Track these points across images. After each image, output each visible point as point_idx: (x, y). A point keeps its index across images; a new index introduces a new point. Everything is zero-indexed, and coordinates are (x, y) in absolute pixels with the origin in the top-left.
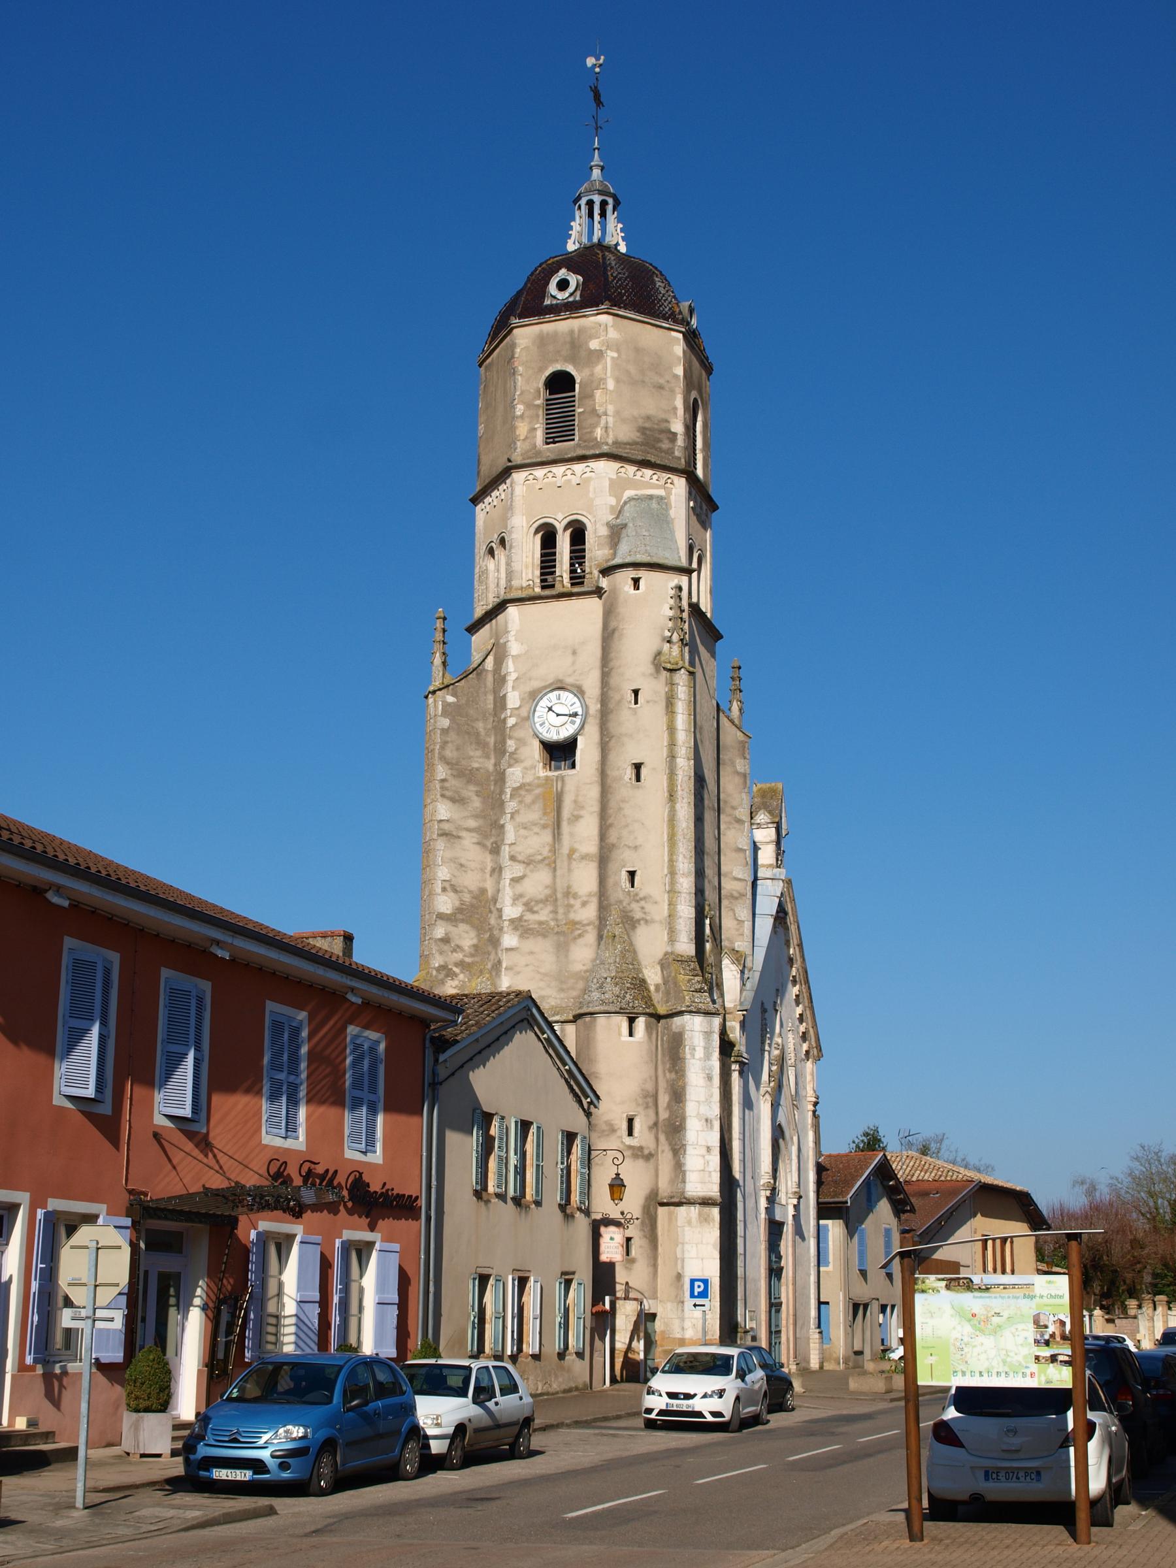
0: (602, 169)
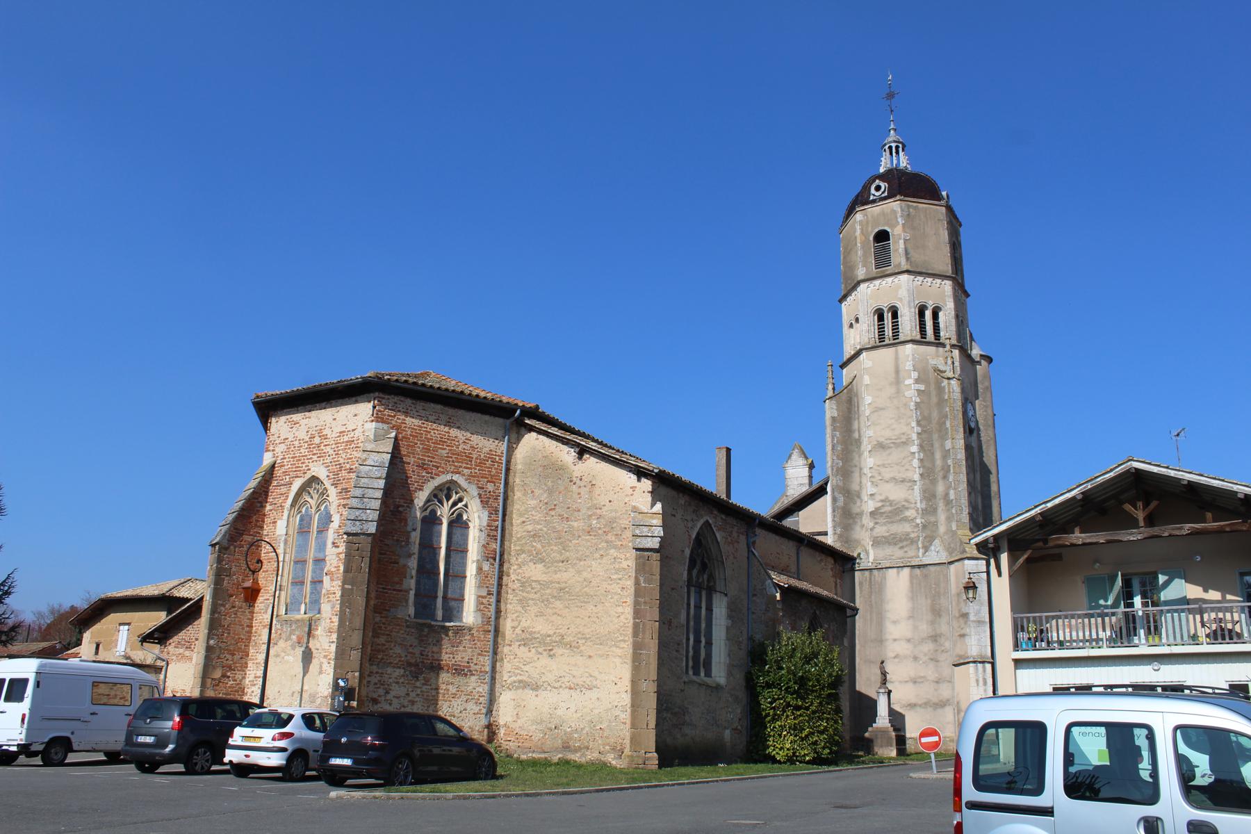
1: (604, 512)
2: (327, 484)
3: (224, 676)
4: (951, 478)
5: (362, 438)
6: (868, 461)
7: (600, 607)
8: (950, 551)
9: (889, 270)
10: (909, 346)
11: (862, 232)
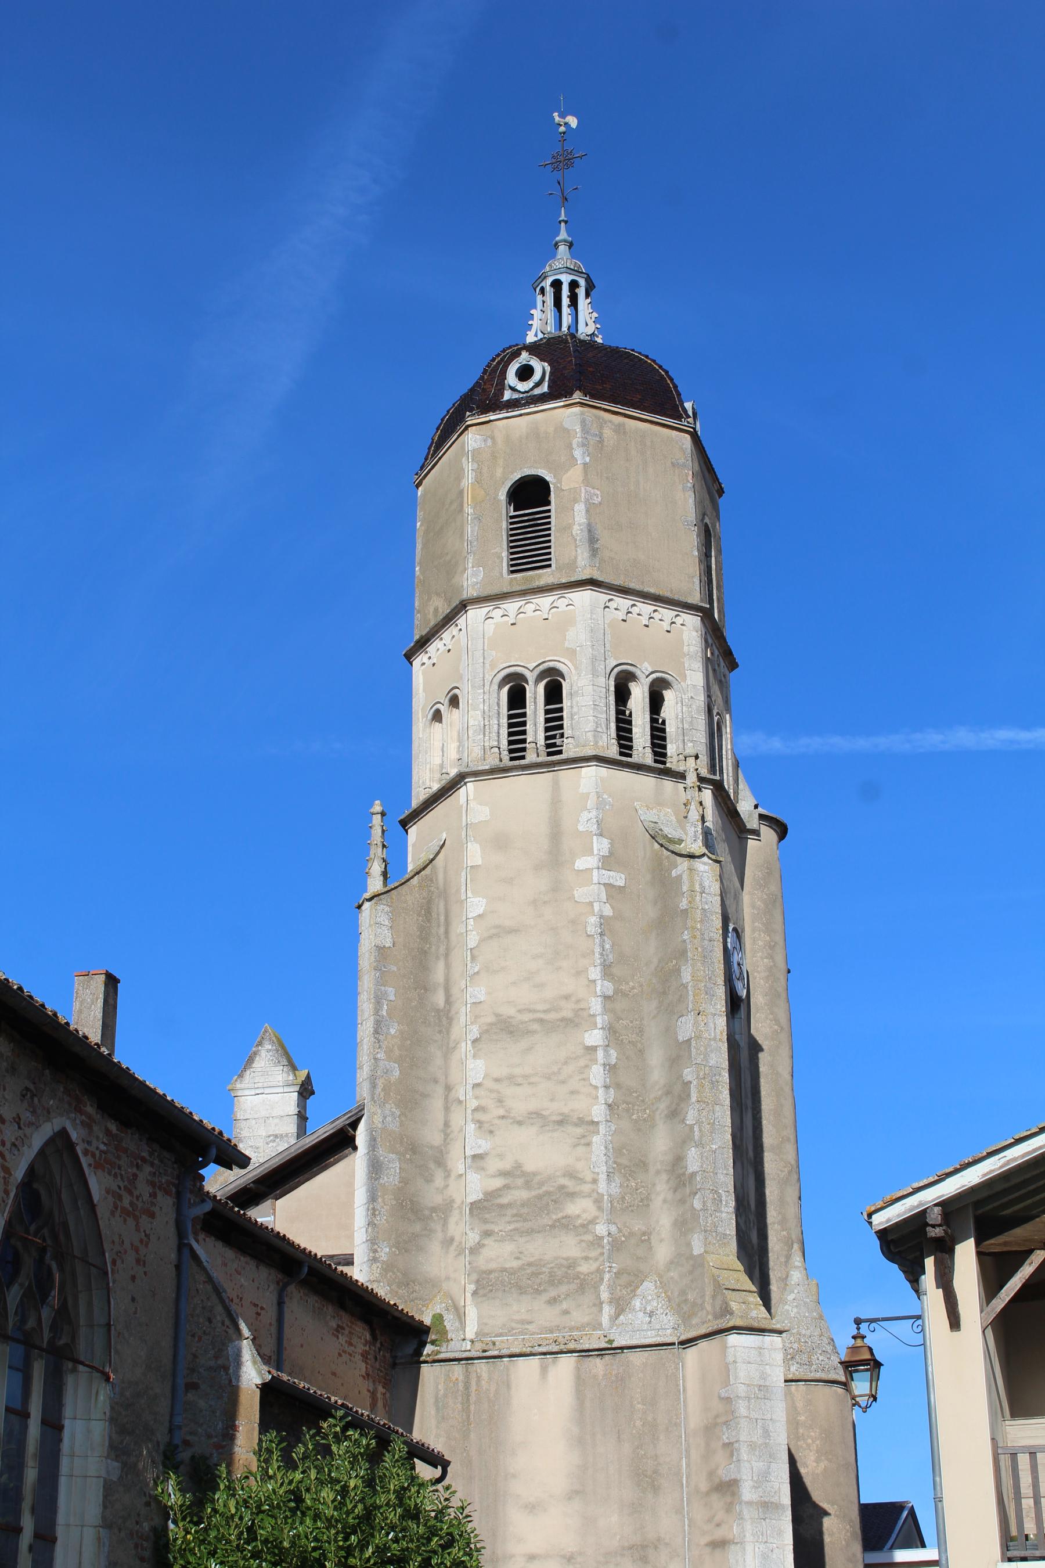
0: (571, 245)
4: (691, 1118)
6: (472, 1068)
8: (684, 1310)
9: (545, 577)
10: (591, 772)
11: (478, 481)
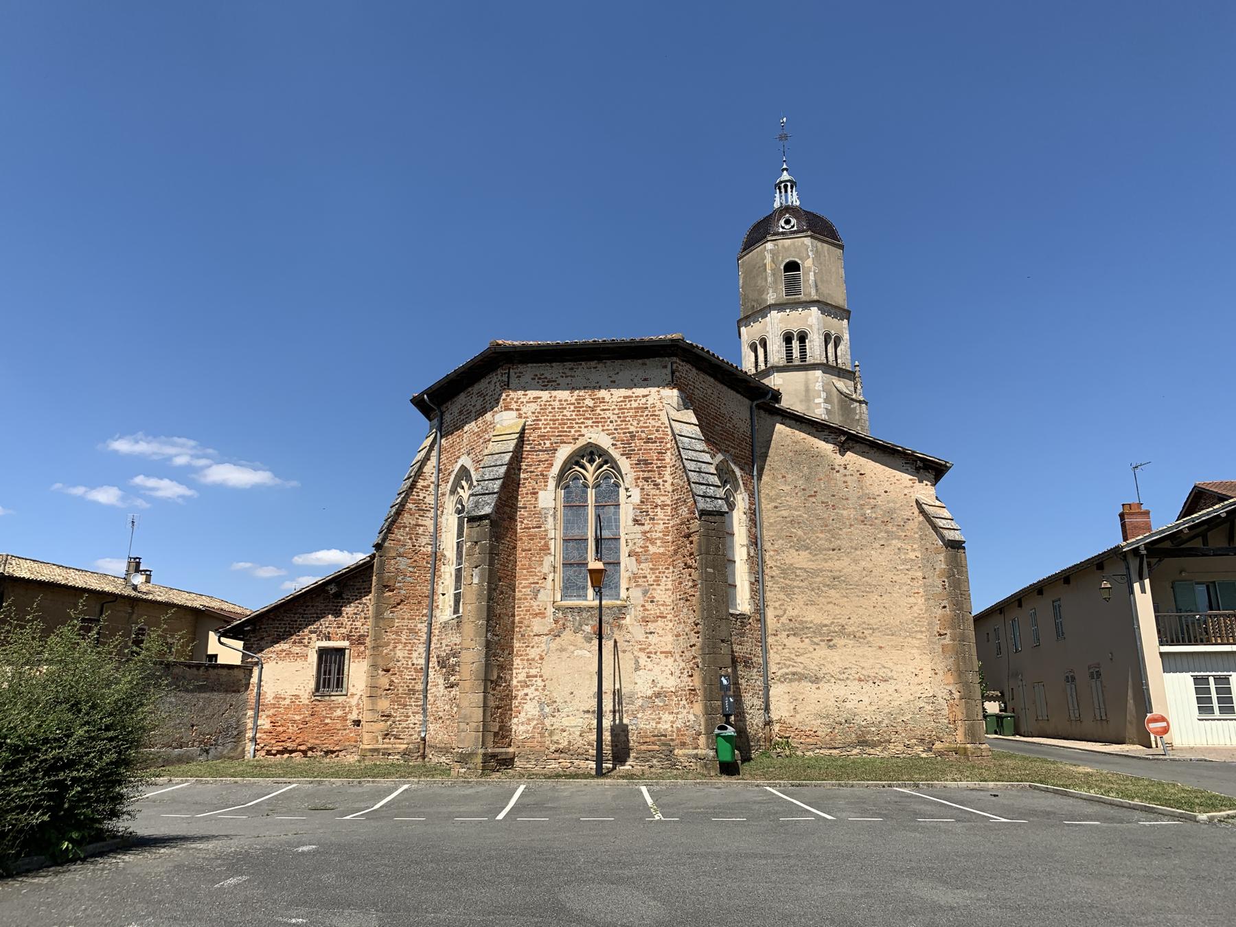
1: (879, 501)
2: (615, 454)
3: (499, 677)
5: (658, 404)
7: (886, 598)
11: (773, 261)
